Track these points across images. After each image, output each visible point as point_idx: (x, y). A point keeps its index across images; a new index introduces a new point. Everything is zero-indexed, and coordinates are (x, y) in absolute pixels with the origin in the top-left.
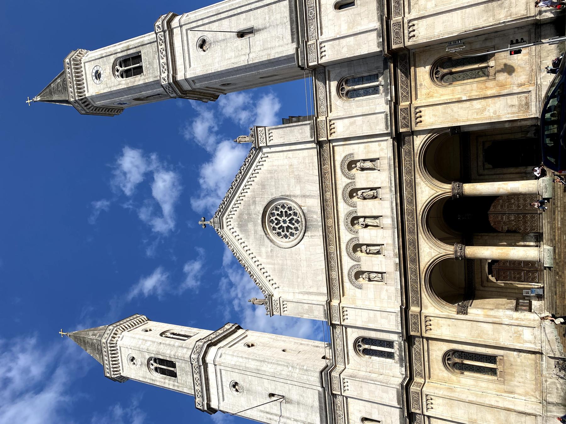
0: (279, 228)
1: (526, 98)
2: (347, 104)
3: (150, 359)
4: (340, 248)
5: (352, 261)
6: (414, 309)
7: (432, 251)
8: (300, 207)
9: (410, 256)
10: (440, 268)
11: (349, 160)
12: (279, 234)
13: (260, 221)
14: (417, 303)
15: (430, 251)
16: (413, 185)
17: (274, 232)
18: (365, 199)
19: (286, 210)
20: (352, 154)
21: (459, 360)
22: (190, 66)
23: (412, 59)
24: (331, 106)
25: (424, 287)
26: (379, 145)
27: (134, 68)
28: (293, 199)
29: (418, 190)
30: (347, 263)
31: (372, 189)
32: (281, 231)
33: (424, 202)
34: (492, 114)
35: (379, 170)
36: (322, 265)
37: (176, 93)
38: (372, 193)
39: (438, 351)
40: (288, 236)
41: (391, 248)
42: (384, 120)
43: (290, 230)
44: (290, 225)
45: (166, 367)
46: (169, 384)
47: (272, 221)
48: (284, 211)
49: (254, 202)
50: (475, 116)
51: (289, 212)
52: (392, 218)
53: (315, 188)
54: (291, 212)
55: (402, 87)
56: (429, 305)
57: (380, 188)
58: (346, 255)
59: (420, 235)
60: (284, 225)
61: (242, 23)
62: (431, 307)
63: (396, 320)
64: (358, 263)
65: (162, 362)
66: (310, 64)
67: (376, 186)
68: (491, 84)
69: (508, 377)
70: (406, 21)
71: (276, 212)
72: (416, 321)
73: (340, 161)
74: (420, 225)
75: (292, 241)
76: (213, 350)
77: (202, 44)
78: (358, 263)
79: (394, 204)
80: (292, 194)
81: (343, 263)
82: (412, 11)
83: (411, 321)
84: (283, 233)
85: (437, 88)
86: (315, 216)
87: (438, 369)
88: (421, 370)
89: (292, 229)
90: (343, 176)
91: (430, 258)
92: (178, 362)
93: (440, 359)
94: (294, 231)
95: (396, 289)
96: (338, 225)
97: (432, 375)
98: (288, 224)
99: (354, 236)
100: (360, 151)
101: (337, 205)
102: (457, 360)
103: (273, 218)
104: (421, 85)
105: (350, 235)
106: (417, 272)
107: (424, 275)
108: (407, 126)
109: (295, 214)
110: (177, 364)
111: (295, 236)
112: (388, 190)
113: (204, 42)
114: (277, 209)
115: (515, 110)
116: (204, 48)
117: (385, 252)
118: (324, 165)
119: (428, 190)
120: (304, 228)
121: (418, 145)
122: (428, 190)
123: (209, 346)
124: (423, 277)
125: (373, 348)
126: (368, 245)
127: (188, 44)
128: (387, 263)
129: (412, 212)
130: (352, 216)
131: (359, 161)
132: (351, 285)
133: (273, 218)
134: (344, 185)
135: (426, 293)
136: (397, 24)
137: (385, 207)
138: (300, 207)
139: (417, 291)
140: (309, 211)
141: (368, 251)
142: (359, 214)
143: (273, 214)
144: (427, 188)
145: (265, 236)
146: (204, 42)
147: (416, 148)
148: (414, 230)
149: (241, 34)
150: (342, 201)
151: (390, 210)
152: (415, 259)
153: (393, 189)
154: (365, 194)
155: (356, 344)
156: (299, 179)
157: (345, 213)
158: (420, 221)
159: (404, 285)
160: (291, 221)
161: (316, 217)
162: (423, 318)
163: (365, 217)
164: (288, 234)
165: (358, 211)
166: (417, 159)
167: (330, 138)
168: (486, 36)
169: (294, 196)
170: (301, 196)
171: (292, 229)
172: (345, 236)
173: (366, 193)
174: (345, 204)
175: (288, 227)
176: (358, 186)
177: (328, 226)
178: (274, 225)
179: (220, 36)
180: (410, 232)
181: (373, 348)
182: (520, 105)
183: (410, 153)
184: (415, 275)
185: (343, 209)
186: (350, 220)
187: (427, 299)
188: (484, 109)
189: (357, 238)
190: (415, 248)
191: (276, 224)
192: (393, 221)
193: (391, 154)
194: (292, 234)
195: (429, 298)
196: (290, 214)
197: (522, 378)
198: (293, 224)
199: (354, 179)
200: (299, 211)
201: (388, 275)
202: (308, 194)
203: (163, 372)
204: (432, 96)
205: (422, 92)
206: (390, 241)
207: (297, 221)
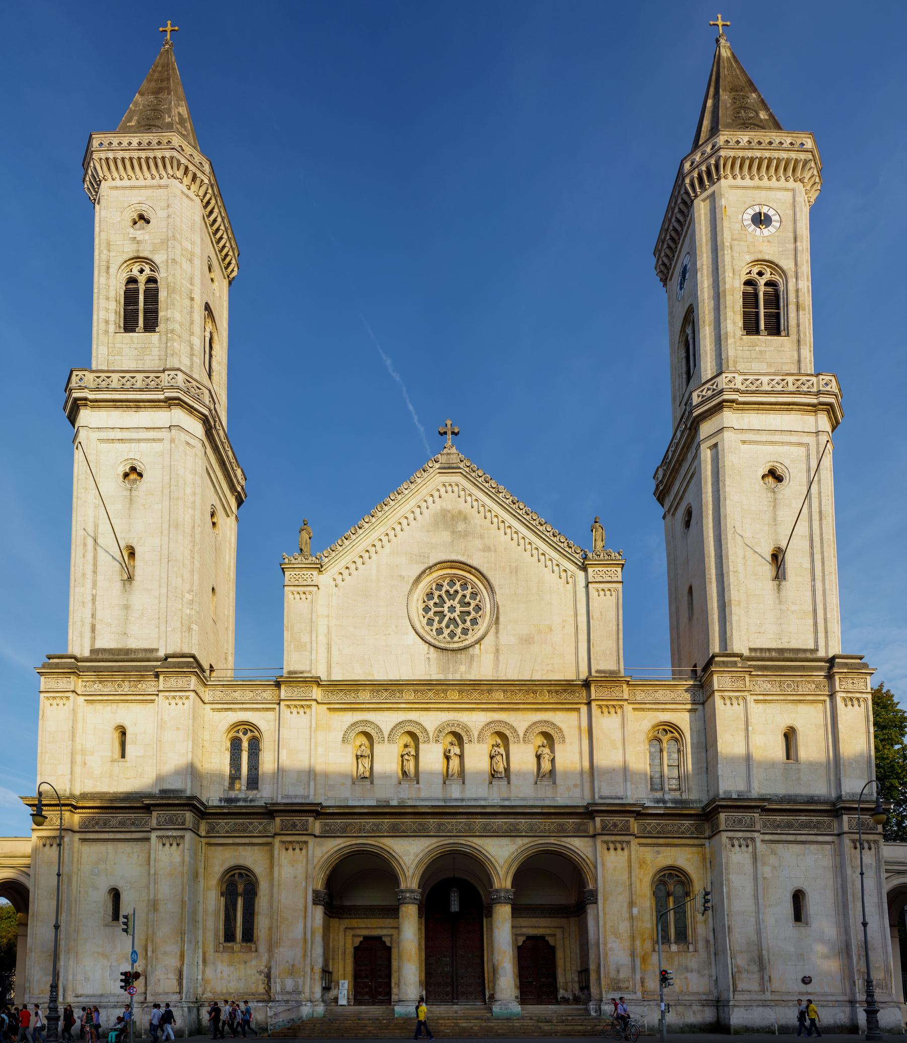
1: (627, 988)
3: (154, 267)
4: (411, 709)
5: (389, 729)
6: (316, 826)
7: (412, 857)
8: (478, 642)
9: (403, 823)
11: (555, 736)
12: (430, 595)
14: (326, 831)
15: (410, 854)
16: (511, 833)
17: (434, 587)
18: (492, 757)
19: (473, 613)
20: (564, 741)
21: (240, 888)
22: (744, 442)
23: (696, 842)
24: (643, 710)
25: (354, 842)
26: (575, 786)
27: (757, 314)
28: (493, 630)
29: (504, 841)
30: (386, 720)
32: (436, 600)
33: (486, 848)
34: (609, 945)
35: (536, 783)
36: (380, 675)
37: (698, 405)
39: (252, 858)
40: (427, 613)
41: (413, 795)
42: (614, 794)
43: (437, 619)
44: (446, 619)
45: (142, 308)
46: (107, 310)
47: (452, 583)
48: (471, 608)
49: (487, 549)
50: (609, 924)
51: (468, 619)
52: (462, 800)
53: (511, 671)
54: (468, 623)
55: (659, 824)
56: (325, 849)
57: (509, 783)
58: (400, 720)
59: (434, 840)
60: (446, 606)
61: (795, 561)
62: (324, 851)
63: (296, 796)
64: (386, 739)
65: (152, 296)
66: (715, 677)
68: (648, 945)
69: (226, 956)
70: (756, 835)
71: (468, 593)
72: (298, 828)
73: (552, 720)
74: (451, 841)
75: (421, 622)
76: (198, 428)
77: (774, 475)
78: (386, 739)
79: (483, 803)
80: (501, 627)
81: (387, 713)
82: (764, 846)
83: (296, 819)
84: (431, 603)
85: (651, 875)
86: (463, 668)
87: (222, 859)
88: (218, 832)
89: (440, 622)
90: (530, 723)
91: (400, 854)
92: (160, 339)
93: (241, 862)
94: (436, 625)
95: (347, 799)
96: (448, 710)
97: (213, 848)
98: (449, 615)
99: (431, 735)
101: (483, 710)
102: (240, 888)
103: (457, 587)
104: (658, 852)
105: (433, 730)
106: (377, 833)
107: (373, 843)
108: (603, 829)
109: (465, 631)
110: (154, 337)
111: (428, 628)
112: (505, 795)
113: (779, 479)
114: (474, 595)
115: (613, 974)
116: (770, 479)
117: (405, 785)
118: (549, 692)
119: (501, 854)
120: (442, 645)
121: (572, 843)
122: (501, 854)
123: (205, 421)
124: (369, 842)
125: (245, 756)
127: (783, 443)
129: (470, 830)
130: (463, 734)
131: (552, 750)
132: (349, 724)
133: (457, 587)
134: (515, 724)
135: (343, 845)
136: (753, 824)
138: (478, 642)
139: (345, 832)
140: (472, 656)
141: (406, 757)
142: (467, 747)
143: (464, 586)
144: (507, 854)
145: (426, 566)
146: (779, 479)
147: (568, 840)
148: (443, 831)
149: (777, 557)
150: (489, 720)
151: (474, 796)
152: (397, 831)
153: (507, 803)
154: (499, 758)
155: (248, 727)
156: (527, 640)
157: (469, 724)
158: (456, 841)
159: (356, 811)
160: (453, 620)
161: (463, 671)
162: (304, 838)
163: (461, 757)
164: (431, 614)
165: (472, 745)
166: (552, 842)
167: (594, 704)
168: (712, 942)
169: (497, 632)
170: (497, 645)
171: (440, 622)
172: (431, 720)
173: (500, 761)
174: (483, 724)
175: (441, 615)
176: (512, 747)
177: (446, 691)
178: (446, 587)
179: (787, 516)
180: (440, 825)
181: (245, 756)
182: (619, 981)
183: (562, 832)
184: (373, 830)
186: (458, 730)
188: (616, 935)
189: (427, 741)
190: (415, 831)
192: (456, 800)
193: (561, 802)
194: (430, 622)
195: (335, 849)
196: (464, 622)
197: (229, 975)
198: (447, 627)
199: (524, 741)
200: (471, 638)
201: (369, 787)
202: (501, 658)
203: (130, 297)
204: (641, 867)
205: (648, 853)
207: (452, 635)
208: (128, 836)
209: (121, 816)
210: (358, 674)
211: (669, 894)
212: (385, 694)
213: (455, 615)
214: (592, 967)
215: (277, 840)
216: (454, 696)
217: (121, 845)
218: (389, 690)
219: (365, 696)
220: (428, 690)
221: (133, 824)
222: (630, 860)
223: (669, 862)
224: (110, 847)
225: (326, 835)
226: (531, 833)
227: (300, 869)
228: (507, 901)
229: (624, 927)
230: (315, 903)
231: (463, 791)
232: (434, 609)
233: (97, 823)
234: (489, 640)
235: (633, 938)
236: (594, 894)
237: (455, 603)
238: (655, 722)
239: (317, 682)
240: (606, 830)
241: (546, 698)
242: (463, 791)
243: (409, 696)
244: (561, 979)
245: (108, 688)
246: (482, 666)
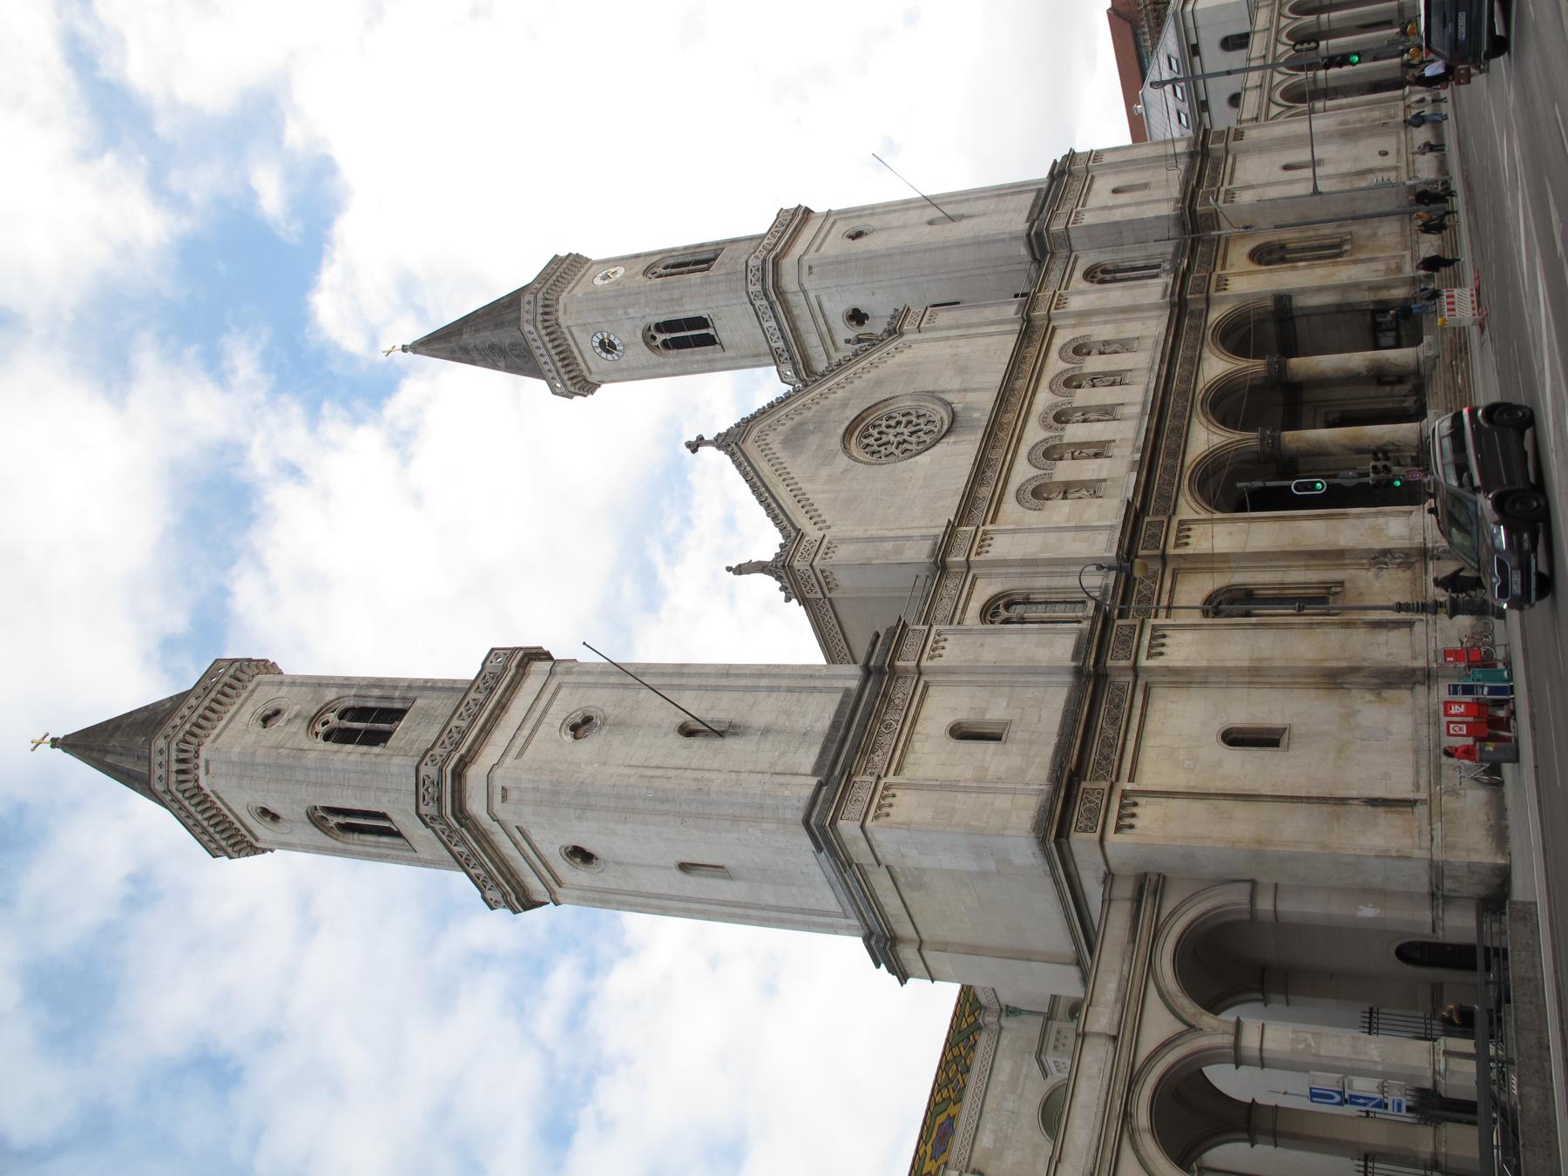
16: (1195, 363)
25: (1186, 482)
101: (1034, 394)
129: (1186, 392)
140: (964, 409)
189: (1061, 437)
208: (1137, 711)
209: (1101, 722)
212: (989, 473)
216: (1009, 417)
217: (1151, 726)
221: (1118, 707)
224: (1149, 743)
225: (1170, 509)
231: (1133, 404)
233: (1107, 758)
234: (948, 397)
239: (952, 529)
241: (1033, 351)
242: (1133, 404)
243: (997, 454)
245: (887, 740)
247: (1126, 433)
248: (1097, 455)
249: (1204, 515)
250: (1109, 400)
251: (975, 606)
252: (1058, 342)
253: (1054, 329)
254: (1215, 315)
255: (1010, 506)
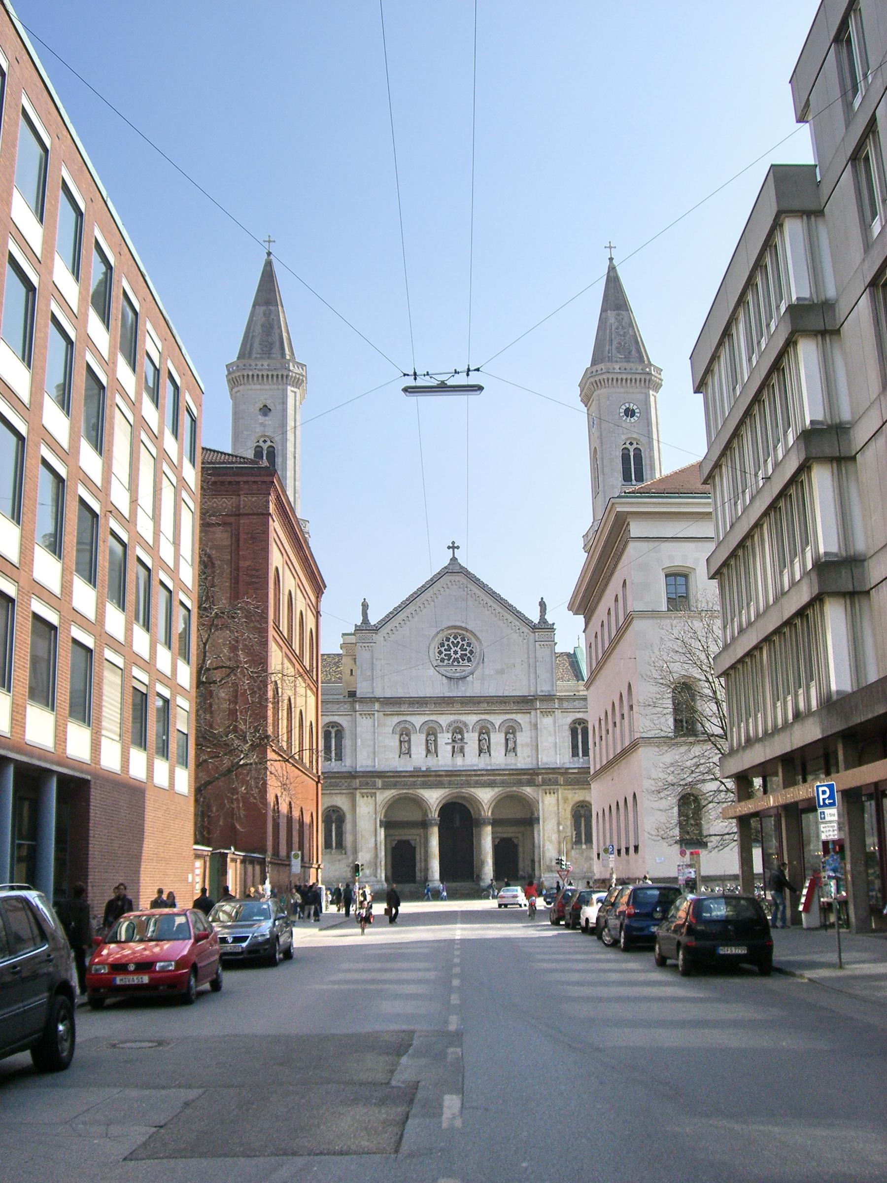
0: (448, 645)
2: (567, 727)
6: (379, 782)
10: (419, 803)
11: (517, 728)
12: (442, 645)
13: (458, 624)
15: (434, 797)
16: (491, 784)
18: (480, 741)
26: (528, 757)
29: (488, 790)
30: (418, 721)
31: (489, 747)
32: (446, 647)
38: (484, 749)
62: (385, 796)
67: (492, 752)
84: (443, 649)
98: (454, 656)
100: (523, 738)
103: (459, 639)
106: (414, 785)
122: (485, 796)
126: (435, 741)
128: (419, 758)
131: (515, 736)
133: (459, 639)
137: (471, 759)
143: (463, 639)
153: (489, 768)
162: (373, 791)
164: (443, 656)
172: (444, 720)
176: (492, 736)
178: (452, 639)
183: (520, 783)
185: (471, 719)
186: (461, 725)
187: (390, 794)
191: (453, 642)
204: (565, 802)
206: (440, 763)
210: (400, 693)
211: (581, 816)
213: (458, 656)
214: (536, 859)
215: (358, 791)
218: (419, 703)
219: (404, 708)
220: (444, 703)
222: (558, 800)
223: (582, 798)
225: (386, 787)
226: (503, 784)
227: (371, 809)
228: (489, 823)
229: (554, 837)
230: (381, 827)
231: (464, 760)
232: (445, 653)
235: (559, 843)
236: (538, 819)
237: (458, 649)
238: (574, 718)
239: (377, 699)
240: (544, 783)
242: (464, 760)
244: (521, 865)
246: (474, 688)
247: (444, 759)
248: (428, 751)
249: (379, 802)
250: (466, 750)
251: (336, 719)
252: (519, 718)
253: (530, 713)
254: (528, 790)
255: (396, 719)
